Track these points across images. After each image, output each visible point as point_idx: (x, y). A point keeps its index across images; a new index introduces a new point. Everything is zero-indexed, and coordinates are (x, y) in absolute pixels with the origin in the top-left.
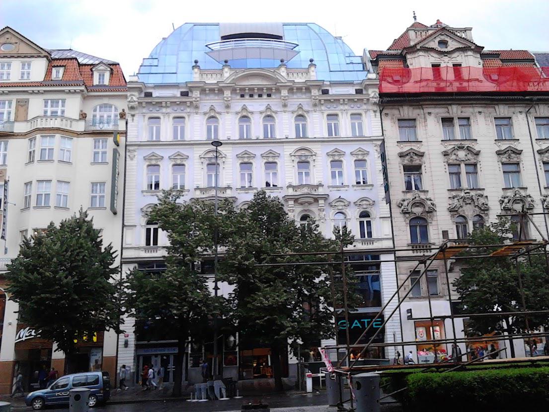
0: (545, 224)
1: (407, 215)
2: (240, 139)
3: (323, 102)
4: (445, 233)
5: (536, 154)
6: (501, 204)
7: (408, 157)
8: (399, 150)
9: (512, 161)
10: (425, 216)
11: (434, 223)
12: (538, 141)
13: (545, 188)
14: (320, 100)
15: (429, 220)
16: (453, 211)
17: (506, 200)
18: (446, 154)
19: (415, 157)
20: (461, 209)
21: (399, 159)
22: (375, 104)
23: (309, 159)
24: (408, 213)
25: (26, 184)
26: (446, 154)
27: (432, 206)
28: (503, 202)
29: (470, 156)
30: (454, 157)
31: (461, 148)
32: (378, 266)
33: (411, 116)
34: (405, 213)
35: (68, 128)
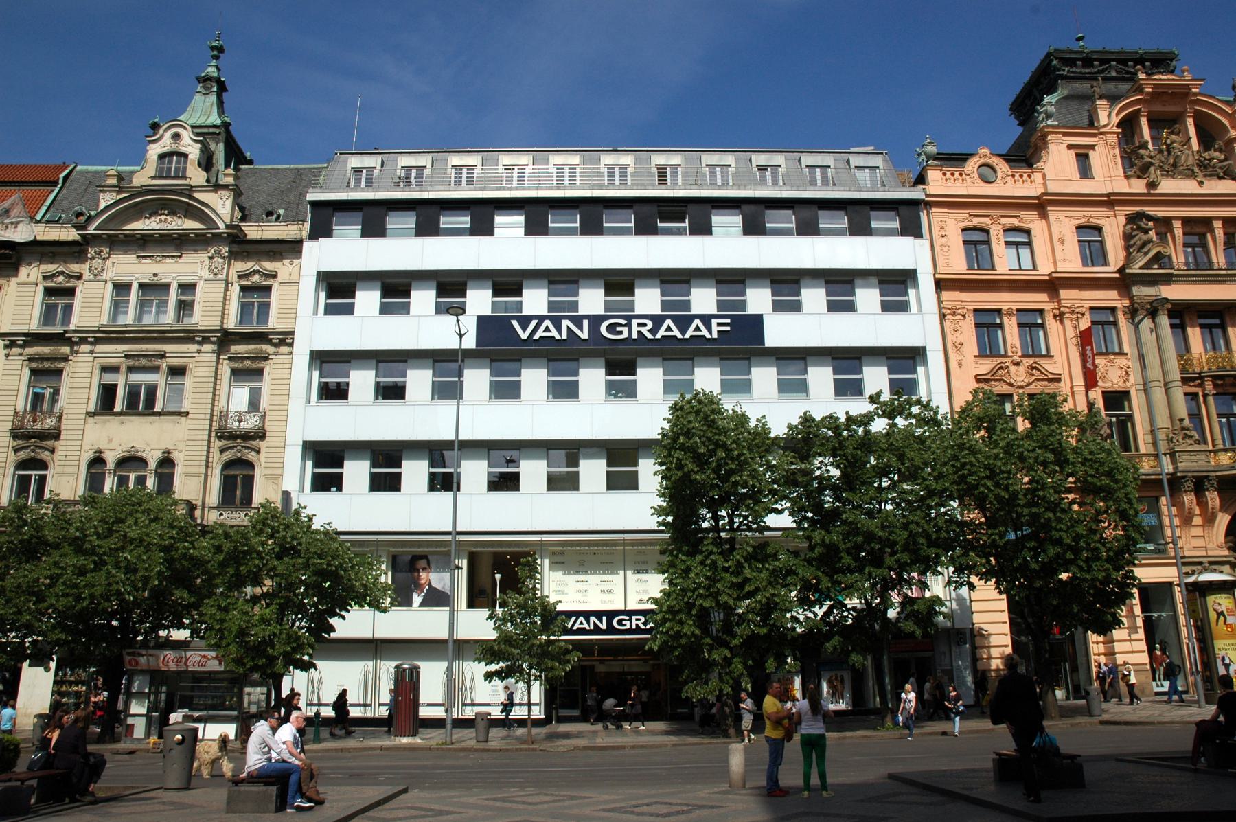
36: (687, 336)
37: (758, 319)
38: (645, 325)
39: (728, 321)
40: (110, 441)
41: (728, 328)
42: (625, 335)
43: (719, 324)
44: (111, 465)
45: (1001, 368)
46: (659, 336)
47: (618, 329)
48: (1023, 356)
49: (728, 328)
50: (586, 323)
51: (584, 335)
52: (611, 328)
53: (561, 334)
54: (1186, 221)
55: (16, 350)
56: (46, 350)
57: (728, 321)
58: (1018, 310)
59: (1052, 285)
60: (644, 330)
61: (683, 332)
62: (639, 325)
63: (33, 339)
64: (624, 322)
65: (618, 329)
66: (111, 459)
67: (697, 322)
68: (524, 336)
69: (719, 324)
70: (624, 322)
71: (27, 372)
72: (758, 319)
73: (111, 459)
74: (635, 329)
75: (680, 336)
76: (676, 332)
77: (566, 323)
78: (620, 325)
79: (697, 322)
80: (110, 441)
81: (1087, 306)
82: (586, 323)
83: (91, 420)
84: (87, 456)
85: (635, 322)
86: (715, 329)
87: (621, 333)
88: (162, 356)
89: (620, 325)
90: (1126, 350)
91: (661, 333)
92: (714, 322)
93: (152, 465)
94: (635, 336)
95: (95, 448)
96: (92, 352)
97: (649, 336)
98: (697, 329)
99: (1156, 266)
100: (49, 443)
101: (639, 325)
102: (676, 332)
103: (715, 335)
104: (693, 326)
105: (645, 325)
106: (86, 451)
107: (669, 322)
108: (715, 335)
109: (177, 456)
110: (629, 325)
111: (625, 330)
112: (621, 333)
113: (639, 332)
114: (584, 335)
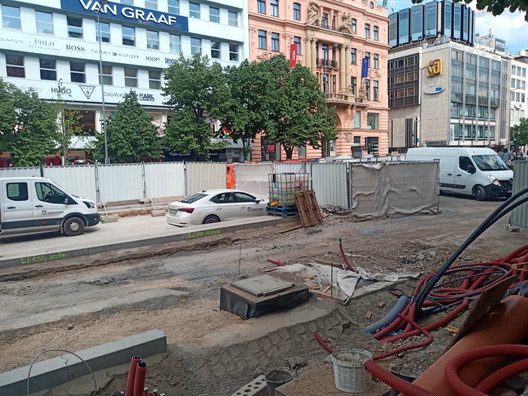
36: (159, 22)
37: (186, 19)
38: (141, 13)
39: (175, 18)
41: (175, 21)
42: (133, 16)
43: (172, 19)
45: (265, 55)
46: (147, 19)
47: (130, 13)
48: (272, 51)
49: (175, 21)
50: (115, 7)
51: (115, 13)
52: (127, 11)
53: (104, 11)
54: (325, 8)
57: (175, 18)
58: (273, 33)
59: (284, 24)
60: (141, 15)
61: (158, 19)
62: (139, 12)
64: (132, 10)
65: (130, 13)
67: (163, 16)
68: (87, 7)
69: (172, 19)
70: (132, 10)
72: (186, 19)
74: (137, 14)
75: (156, 21)
76: (154, 19)
77: (106, 6)
78: (131, 11)
79: (163, 16)
81: (294, 35)
82: (115, 7)
85: (137, 11)
86: (170, 21)
87: (131, 15)
89: (131, 11)
90: (302, 54)
91: (148, 18)
92: (170, 17)
94: (137, 17)
97: (143, 19)
98: (163, 19)
99: (315, 24)
101: (139, 12)
102: (154, 19)
103: (170, 24)
104: (161, 18)
105: (141, 13)
107: (151, 14)
108: (170, 24)
110: (134, 12)
111: (133, 14)
112: (131, 15)
113: (139, 16)
114: (115, 13)
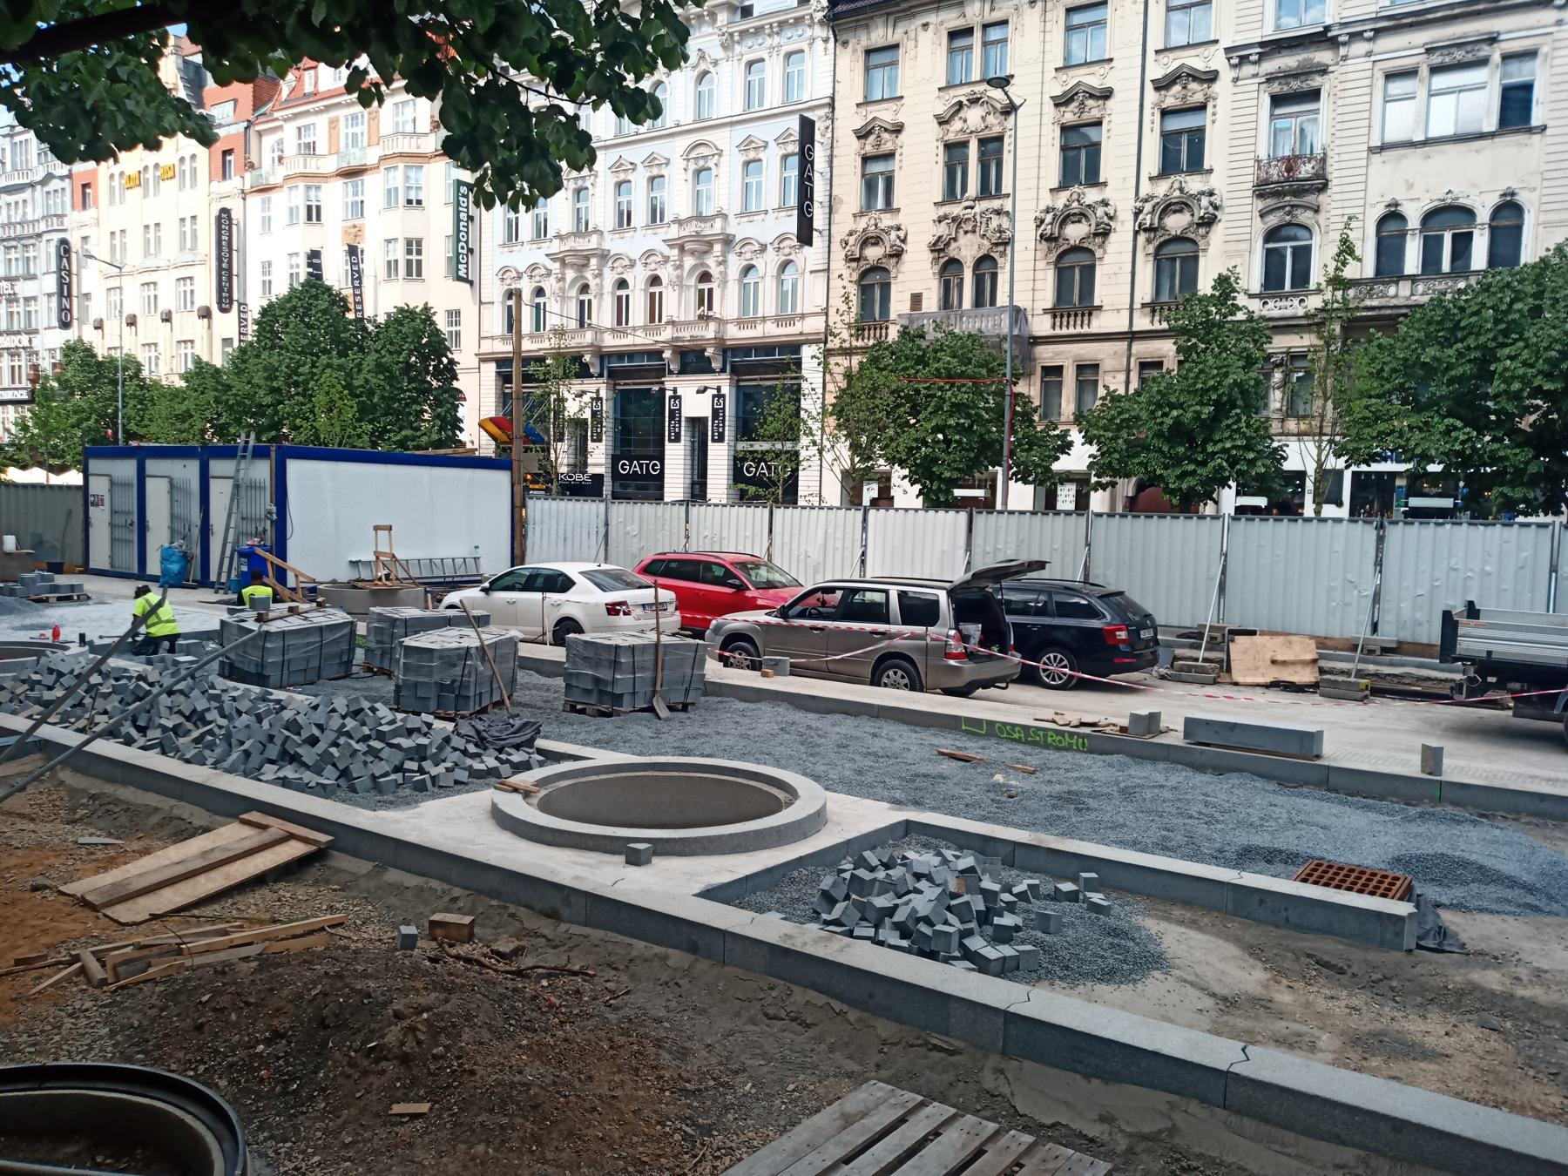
0: (1129, 268)
1: (854, 265)
2: (616, 137)
3: (736, 38)
4: (916, 300)
5: (1149, 87)
6: (1038, 226)
7: (872, 138)
8: (859, 123)
9: (1086, 117)
10: (885, 263)
11: (900, 277)
12: (1161, 56)
13: (1151, 179)
14: (731, 35)
15: (1098, 254)
16: (938, 247)
17: (1049, 218)
18: (943, 121)
19: (886, 136)
20: (953, 245)
21: (856, 144)
22: (821, 23)
23: (711, 164)
24: (857, 260)
25: (389, 241)
26: (943, 121)
27: (1106, 219)
28: (1042, 221)
29: (991, 119)
30: (957, 125)
31: (974, 101)
32: (798, 364)
33: (891, 40)
34: (850, 259)
35: (414, 150)
40: (1410, 186)
44: (1414, 222)
55: (1248, 70)
56: (1289, 61)
63: (1273, 47)
66: (1414, 215)
71: (1266, 100)
73: (1414, 215)
80: (1410, 186)
83: (1376, 158)
84: (1380, 211)
88: (1492, 40)
93: (1483, 216)
95: (1388, 199)
96: (1369, 54)
100: (1310, 199)
106: (1374, 205)
109: (1522, 198)
